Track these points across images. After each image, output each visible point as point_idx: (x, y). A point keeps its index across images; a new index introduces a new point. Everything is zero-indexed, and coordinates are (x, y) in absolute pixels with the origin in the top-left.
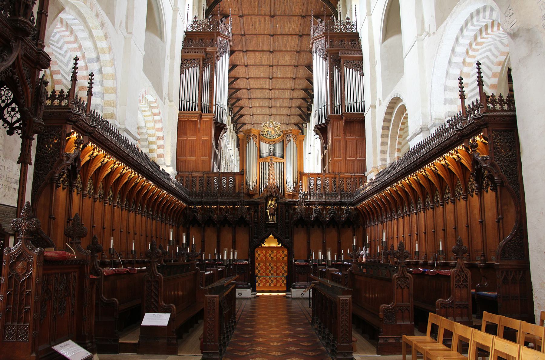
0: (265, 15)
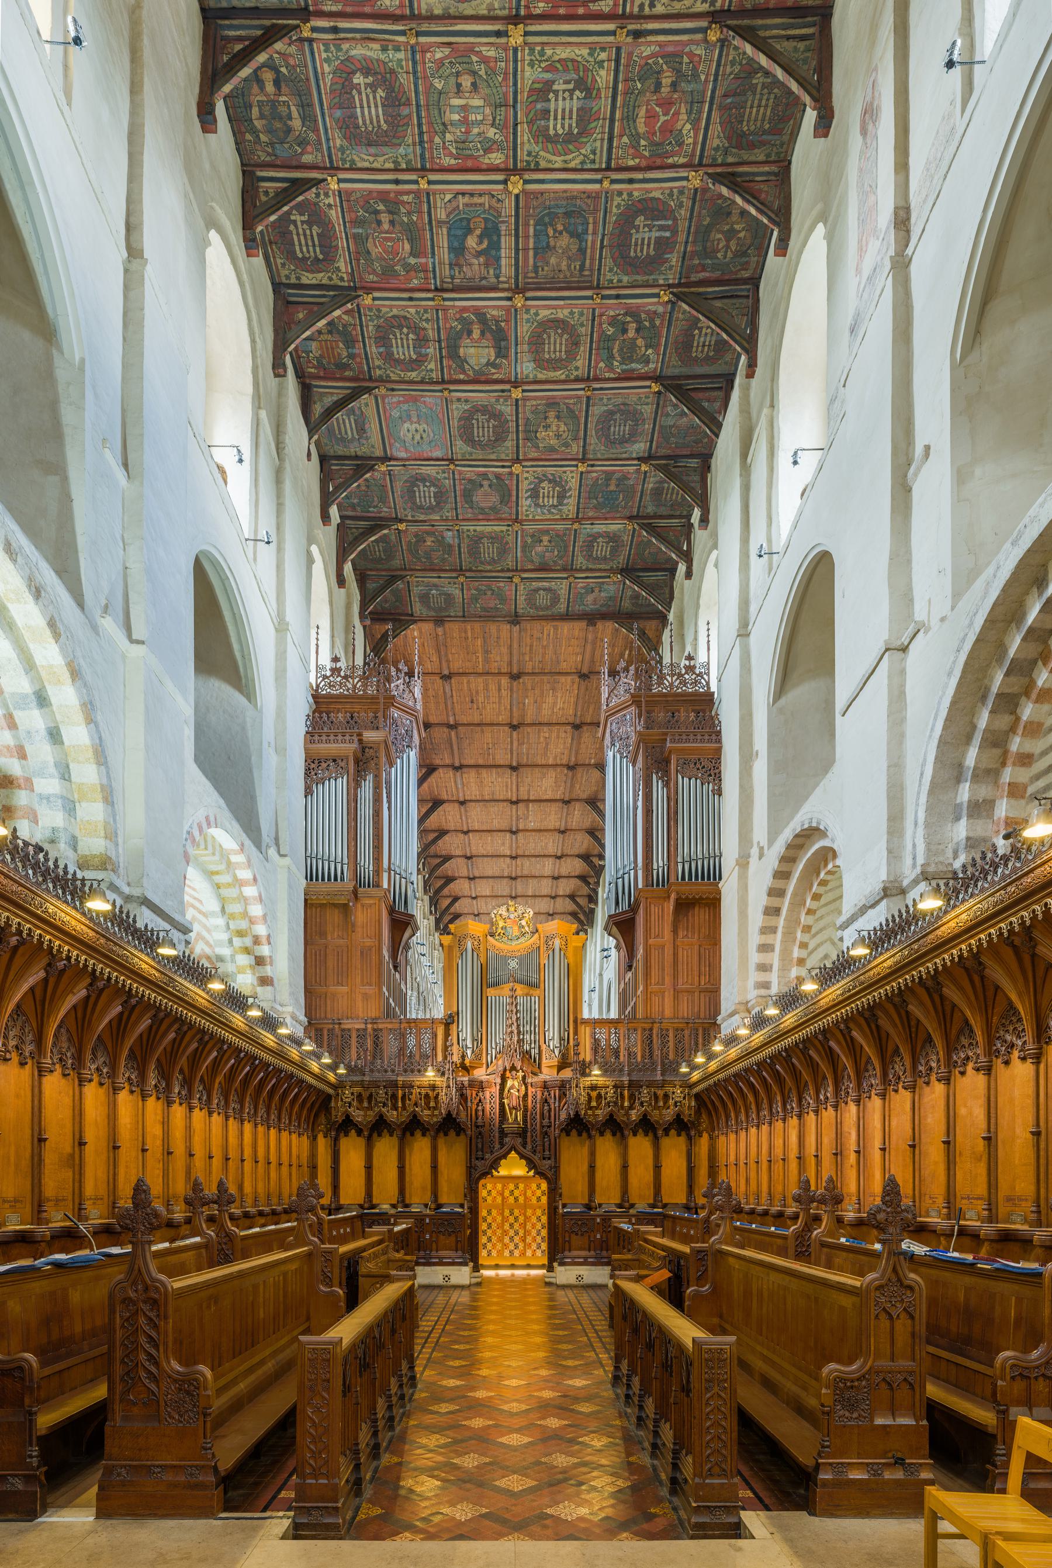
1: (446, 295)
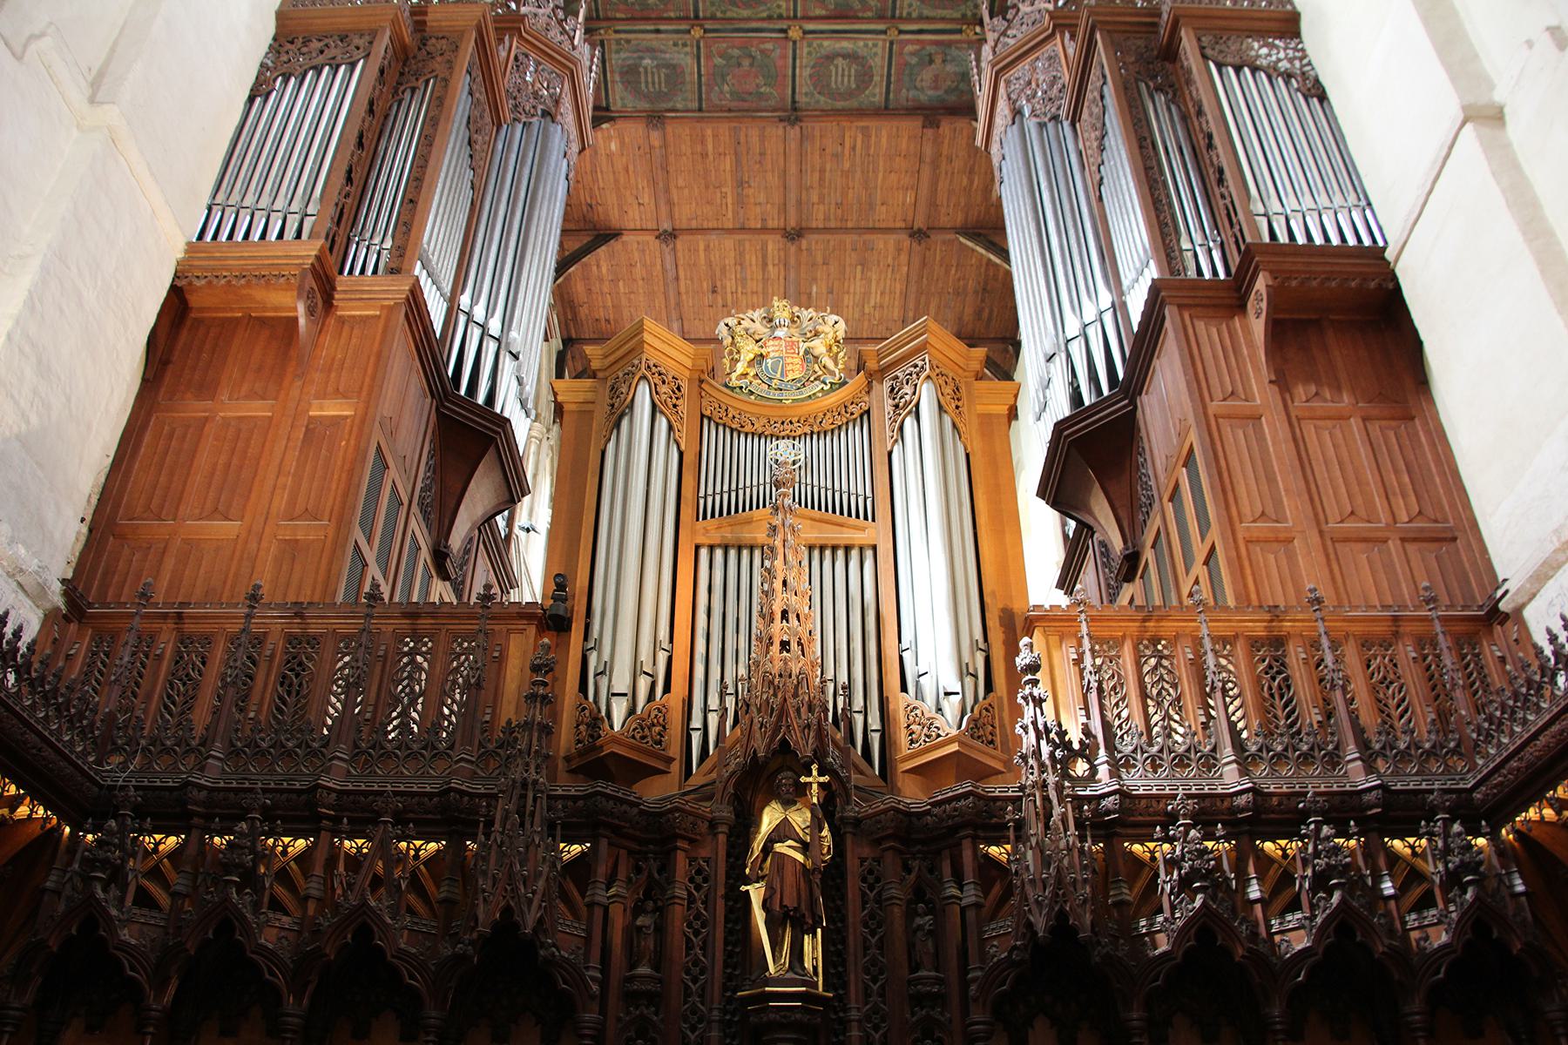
0: (765, 230)
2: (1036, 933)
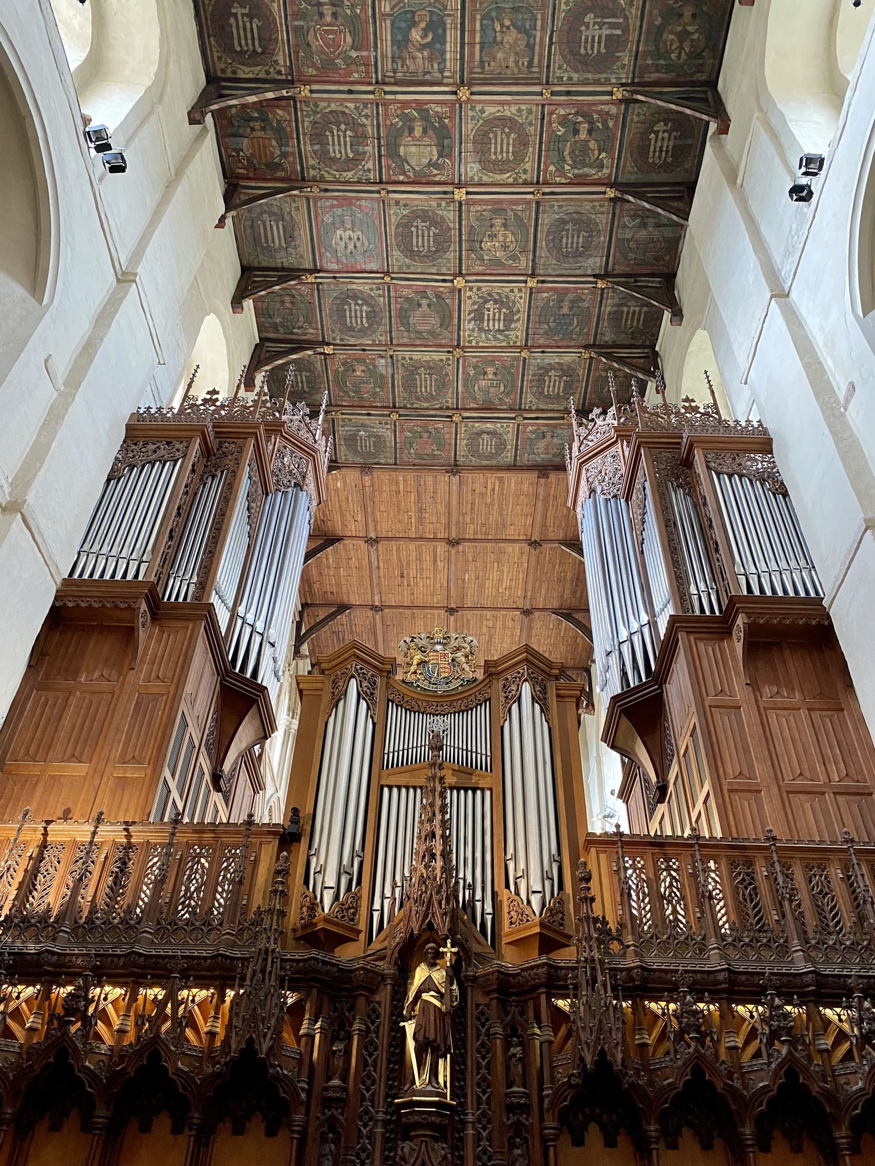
0: (435, 539)
1: (387, 89)
2: (585, 1065)
